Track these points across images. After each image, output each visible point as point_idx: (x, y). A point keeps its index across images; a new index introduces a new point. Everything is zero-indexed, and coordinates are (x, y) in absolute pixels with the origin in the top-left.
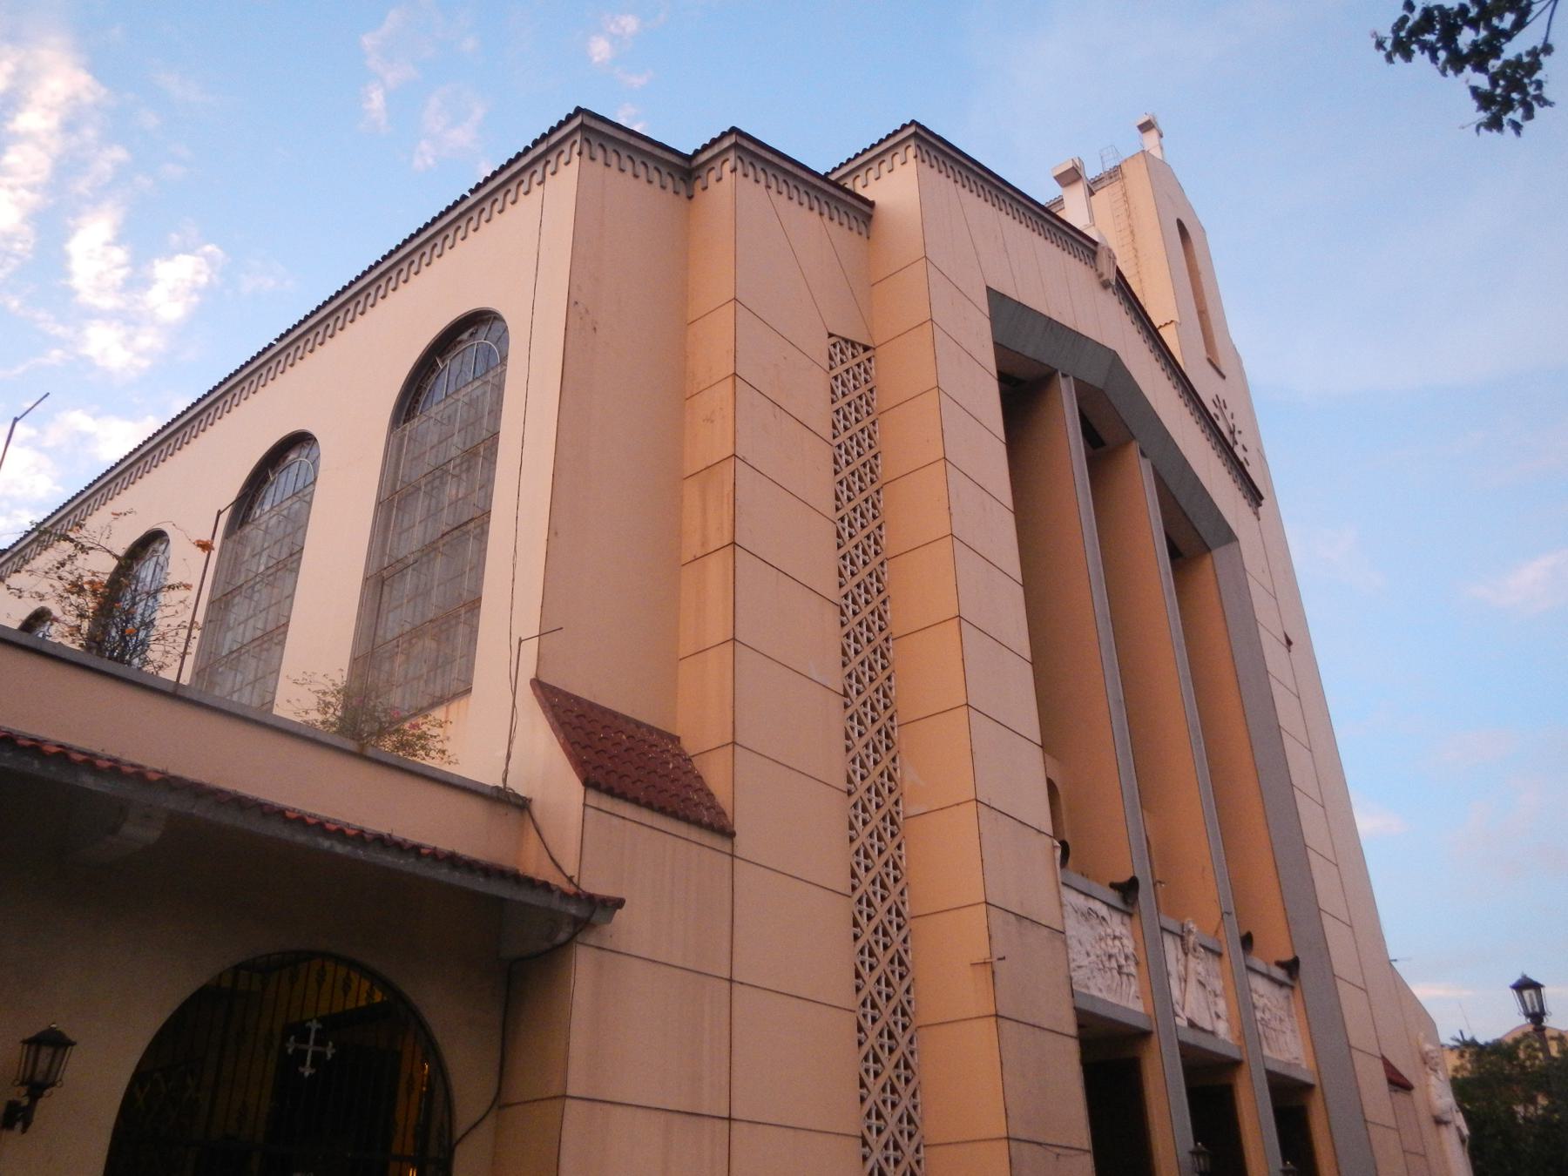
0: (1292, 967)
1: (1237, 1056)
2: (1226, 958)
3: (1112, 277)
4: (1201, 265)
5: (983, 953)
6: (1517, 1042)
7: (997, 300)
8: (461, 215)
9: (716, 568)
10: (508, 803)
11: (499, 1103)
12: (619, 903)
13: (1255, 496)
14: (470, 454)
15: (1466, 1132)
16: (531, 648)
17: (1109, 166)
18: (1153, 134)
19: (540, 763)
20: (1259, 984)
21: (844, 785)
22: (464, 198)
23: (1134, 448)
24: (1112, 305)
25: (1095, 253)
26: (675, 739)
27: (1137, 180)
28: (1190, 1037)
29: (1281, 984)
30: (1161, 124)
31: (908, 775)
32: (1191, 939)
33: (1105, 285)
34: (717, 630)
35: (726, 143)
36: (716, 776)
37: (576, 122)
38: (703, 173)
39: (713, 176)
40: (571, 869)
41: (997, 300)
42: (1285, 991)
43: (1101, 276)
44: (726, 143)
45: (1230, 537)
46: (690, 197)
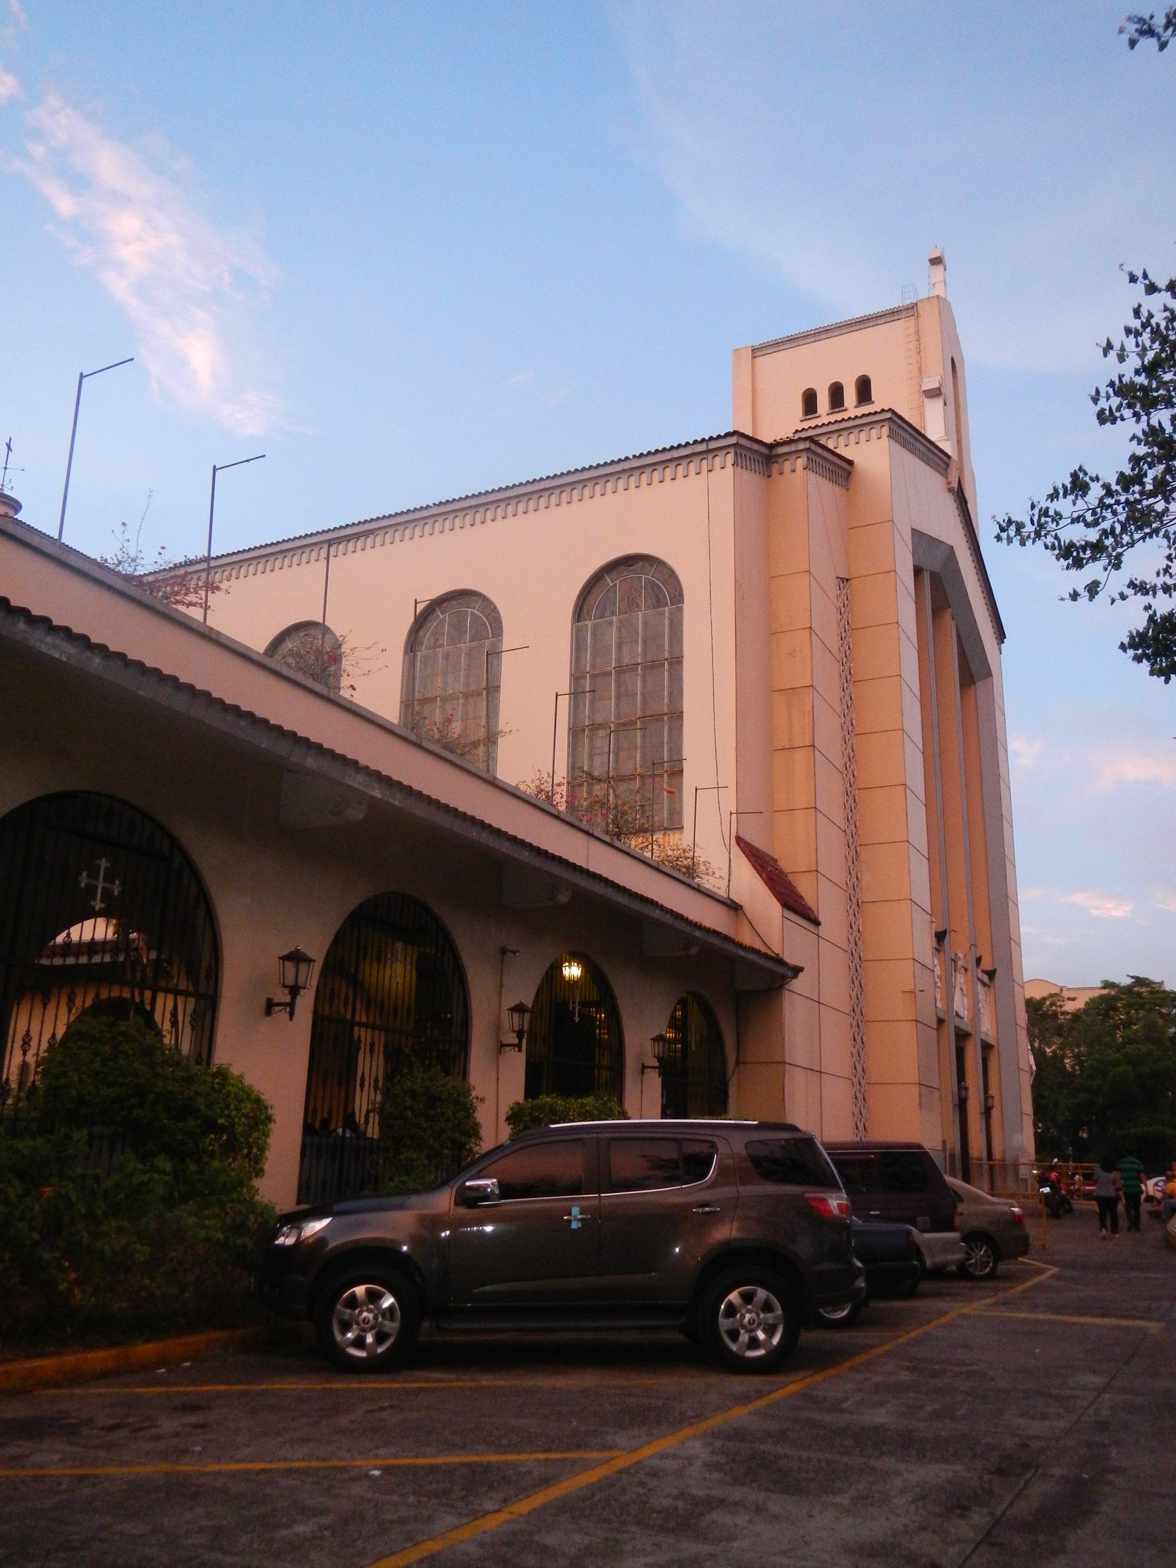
0: (991, 974)
1: (969, 1030)
2: (970, 973)
3: (955, 485)
4: (961, 400)
5: (909, 987)
6: (1044, 999)
7: (914, 531)
8: (624, 471)
9: (800, 759)
10: (734, 907)
11: (738, 1063)
12: (801, 969)
13: (1001, 635)
14: (653, 666)
15: (1034, 1068)
16: (734, 816)
17: (907, 302)
18: (940, 268)
19: (747, 885)
20: (980, 986)
21: (845, 887)
22: (627, 458)
23: (949, 611)
24: (949, 505)
25: (947, 465)
26: (776, 861)
27: (929, 317)
28: (958, 1022)
29: (985, 985)
30: (947, 260)
31: (866, 878)
32: (960, 963)
33: (950, 490)
34: (803, 801)
35: (801, 446)
36: (805, 888)
37: (733, 440)
38: (780, 460)
39: (787, 466)
40: (777, 949)
41: (914, 531)
42: (986, 989)
43: (949, 483)
44: (801, 446)
45: (988, 674)
46: (769, 476)
